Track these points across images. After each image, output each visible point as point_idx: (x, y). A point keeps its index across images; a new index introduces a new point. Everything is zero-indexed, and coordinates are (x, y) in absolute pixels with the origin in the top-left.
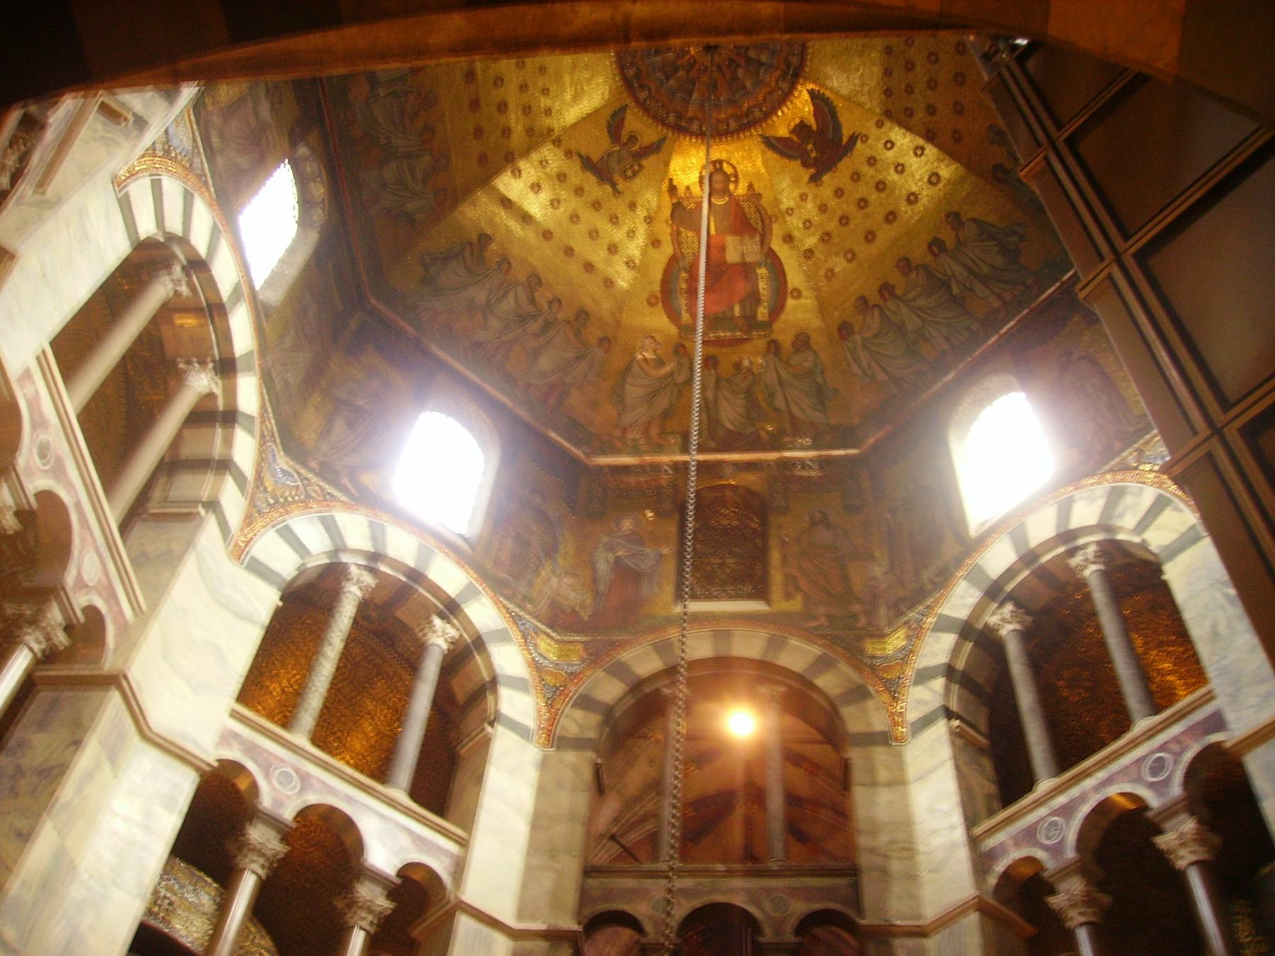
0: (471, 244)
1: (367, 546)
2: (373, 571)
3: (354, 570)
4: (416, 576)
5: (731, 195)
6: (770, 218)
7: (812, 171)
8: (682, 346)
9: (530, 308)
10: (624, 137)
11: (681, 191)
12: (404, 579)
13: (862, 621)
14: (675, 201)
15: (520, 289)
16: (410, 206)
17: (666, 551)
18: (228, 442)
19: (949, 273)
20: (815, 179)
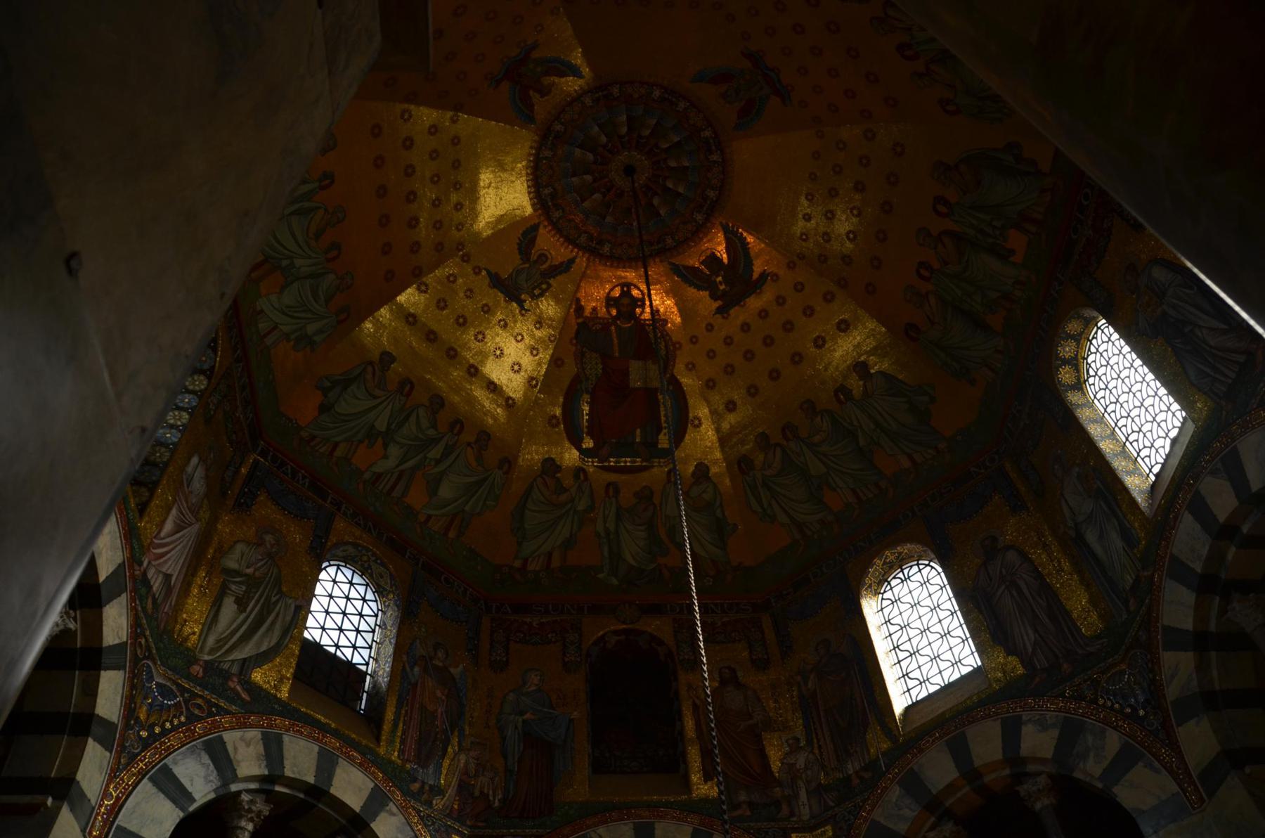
0: (371, 363)
1: (258, 769)
2: (269, 795)
3: (245, 797)
4: (318, 792)
5: (637, 320)
6: (674, 345)
7: (719, 303)
8: (583, 470)
9: (431, 432)
10: (534, 257)
11: (587, 312)
12: (302, 796)
13: (785, 810)
14: (580, 320)
15: (422, 412)
16: (310, 329)
17: (575, 715)
18: (91, 692)
19: (855, 423)
20: (719, 311)
